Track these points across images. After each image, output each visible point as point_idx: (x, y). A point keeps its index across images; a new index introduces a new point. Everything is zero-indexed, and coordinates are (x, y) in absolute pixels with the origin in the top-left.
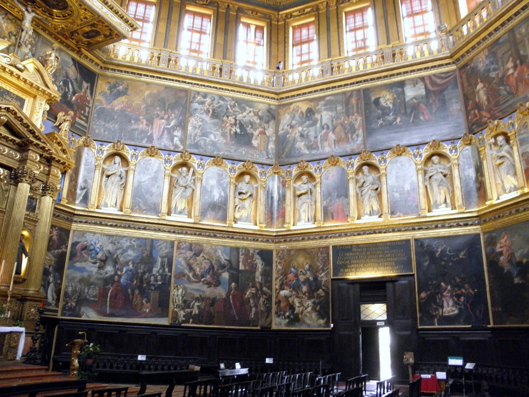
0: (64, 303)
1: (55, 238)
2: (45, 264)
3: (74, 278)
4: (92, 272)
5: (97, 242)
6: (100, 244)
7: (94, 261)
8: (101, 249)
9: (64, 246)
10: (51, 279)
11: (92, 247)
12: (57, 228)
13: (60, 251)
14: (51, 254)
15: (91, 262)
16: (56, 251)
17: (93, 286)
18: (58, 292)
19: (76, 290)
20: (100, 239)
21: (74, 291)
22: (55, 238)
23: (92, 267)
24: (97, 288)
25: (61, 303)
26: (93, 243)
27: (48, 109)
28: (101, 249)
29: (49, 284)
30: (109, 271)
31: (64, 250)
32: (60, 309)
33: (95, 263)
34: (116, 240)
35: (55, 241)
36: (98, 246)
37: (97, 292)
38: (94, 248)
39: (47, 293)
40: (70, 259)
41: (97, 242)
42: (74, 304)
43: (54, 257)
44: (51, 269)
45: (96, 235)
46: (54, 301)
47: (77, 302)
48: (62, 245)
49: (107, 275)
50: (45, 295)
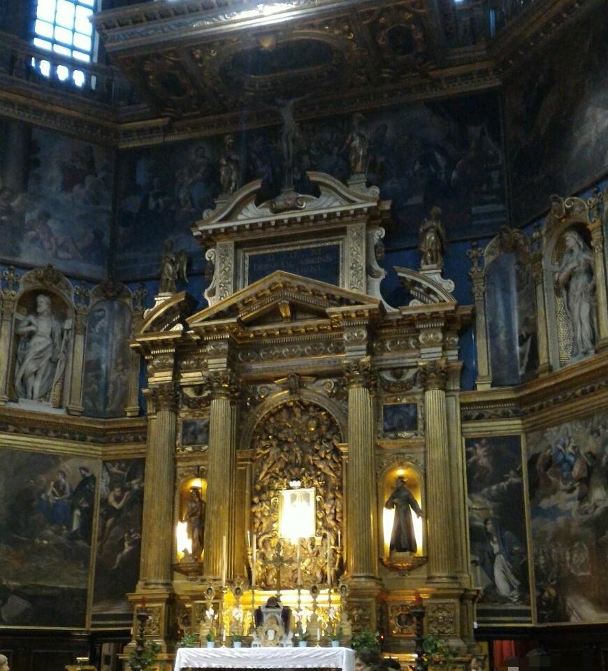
0: (538, 594)
1: (483, 461)
2: (471, 519)
3: (545, 533)
4: (569, 512)
5: (567, 442)
6: (572, 444)
7: (568, 487)
8: (577, 455)
9: (512, 472)
10: (496, 548)
11: (561, 457)
12: (484, 441)
13: (504, 484)
14: (484, 496)
15: (564, 490)
16: (494, 487)
17: (576, 545)
18: (520, 572)
19: (551, 561)
20: (570, 434)
21: (550, 563)
22: (483, 461)
23: (569, 500)
24: (585, 547)
25: (533, 594)
26: (560, 447)
27: (382, 237)
28: (577, 455)
29: (492, 557)
30: (598, 500)
31: (515, 480)
32: (533, 608)
33: (570, 491)
34: (599, 423)
35: (484, 468)
36: (570, 449)
37: (587, 554)
38: (565, 457)
39: (492, 576)
40: (532, 495)
41: (567, 442)
42: (553, 592)
43: (492, 499)
44: (490, 527)
45: (563, 427)
46: (515, 592)
47: (557, 587)
48: (509, 473)
49: (598, 511)
50: (490, 582)
